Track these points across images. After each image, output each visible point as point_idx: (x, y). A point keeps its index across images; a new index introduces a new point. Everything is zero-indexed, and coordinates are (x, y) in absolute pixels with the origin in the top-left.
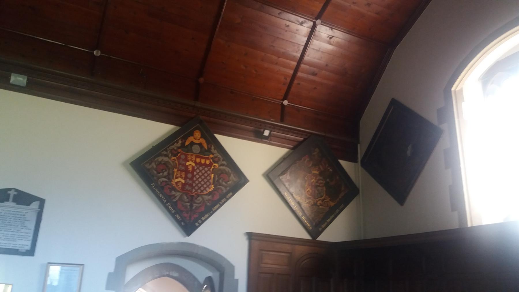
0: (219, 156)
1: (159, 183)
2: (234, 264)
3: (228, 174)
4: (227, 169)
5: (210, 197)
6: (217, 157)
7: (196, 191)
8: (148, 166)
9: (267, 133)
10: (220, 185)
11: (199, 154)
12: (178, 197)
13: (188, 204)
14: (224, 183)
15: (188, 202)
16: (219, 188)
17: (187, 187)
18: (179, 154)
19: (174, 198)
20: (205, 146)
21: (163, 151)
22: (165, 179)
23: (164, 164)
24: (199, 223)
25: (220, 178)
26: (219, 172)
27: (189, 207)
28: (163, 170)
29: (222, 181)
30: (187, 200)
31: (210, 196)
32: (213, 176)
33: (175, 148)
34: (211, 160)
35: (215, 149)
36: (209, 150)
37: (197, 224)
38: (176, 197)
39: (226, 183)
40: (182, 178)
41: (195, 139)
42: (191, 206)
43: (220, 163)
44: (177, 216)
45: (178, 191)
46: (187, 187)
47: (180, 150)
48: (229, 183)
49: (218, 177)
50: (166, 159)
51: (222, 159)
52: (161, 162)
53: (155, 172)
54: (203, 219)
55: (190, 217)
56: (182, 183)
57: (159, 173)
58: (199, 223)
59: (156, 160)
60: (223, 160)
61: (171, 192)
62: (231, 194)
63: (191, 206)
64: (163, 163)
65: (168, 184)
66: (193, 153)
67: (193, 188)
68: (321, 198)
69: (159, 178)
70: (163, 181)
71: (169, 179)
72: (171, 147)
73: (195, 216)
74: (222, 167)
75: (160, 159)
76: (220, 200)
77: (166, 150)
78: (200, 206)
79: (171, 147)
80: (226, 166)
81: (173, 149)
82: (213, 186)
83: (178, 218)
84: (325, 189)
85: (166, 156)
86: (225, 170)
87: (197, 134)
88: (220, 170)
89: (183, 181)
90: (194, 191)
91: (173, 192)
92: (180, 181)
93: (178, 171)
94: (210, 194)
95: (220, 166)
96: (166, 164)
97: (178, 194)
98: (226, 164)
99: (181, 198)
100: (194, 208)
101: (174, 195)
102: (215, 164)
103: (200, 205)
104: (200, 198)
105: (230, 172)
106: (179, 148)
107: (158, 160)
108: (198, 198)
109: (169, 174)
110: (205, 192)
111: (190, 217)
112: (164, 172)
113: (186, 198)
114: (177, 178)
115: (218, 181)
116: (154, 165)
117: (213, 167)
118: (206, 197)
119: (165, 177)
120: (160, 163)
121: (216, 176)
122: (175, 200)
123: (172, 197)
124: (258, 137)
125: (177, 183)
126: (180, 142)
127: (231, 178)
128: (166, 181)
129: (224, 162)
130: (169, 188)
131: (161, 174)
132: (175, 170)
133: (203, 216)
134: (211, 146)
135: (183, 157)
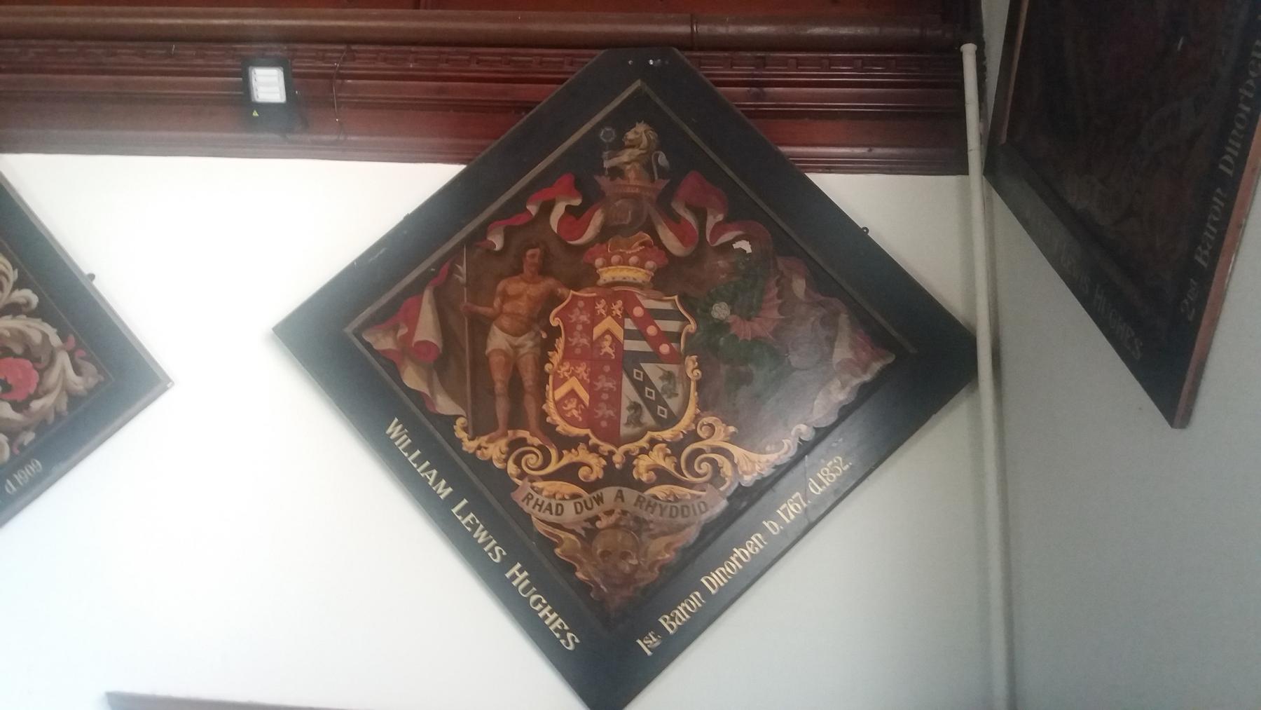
3: (39, 359)
4: (36, 330)
9: (268, 84)
39: (16, 406)
48: (36, 405)
51: (13, 275)
60: (19, 285)
62: (36, 466)
68: (667, 434)
80: (32, 314)
84: (693, 373)
86: (21, 336)
98: (35, 300)
105: (55, 340)
124: (225, 120)
127: (53, 377)
129: (27, 295)
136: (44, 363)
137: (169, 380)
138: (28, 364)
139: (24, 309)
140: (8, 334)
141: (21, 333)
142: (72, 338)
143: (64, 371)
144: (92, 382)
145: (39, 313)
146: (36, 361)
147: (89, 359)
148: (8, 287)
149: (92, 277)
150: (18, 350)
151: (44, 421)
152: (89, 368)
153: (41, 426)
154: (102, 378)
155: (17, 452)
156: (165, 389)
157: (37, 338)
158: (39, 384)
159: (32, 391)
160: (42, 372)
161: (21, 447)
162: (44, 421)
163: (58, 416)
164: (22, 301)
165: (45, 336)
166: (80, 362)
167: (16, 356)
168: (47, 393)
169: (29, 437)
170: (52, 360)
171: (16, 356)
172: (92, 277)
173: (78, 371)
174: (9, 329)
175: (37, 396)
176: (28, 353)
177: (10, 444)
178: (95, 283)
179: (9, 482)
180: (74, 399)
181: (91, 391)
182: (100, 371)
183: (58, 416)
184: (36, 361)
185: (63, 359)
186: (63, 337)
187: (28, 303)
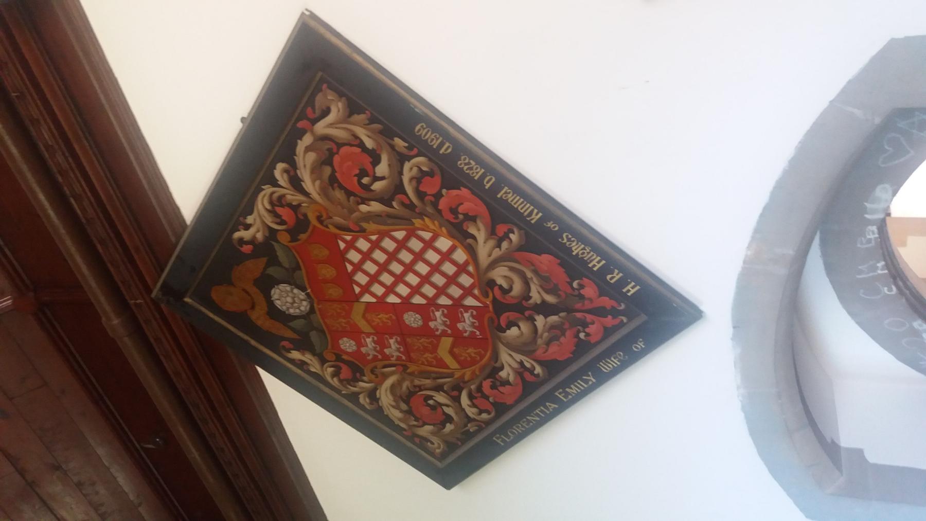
0: (262, 203)
1: (484, 416)
2: (889, 38)
3: (329, 150)
4: (305, 160)
5: (479, 232)
6: (272, 212)
7: (468, 292)
8: (437, 445)
10: (399, 188)
11: (303, 289)
12: (519, 357)
13: (540, 320)
14: (382, 169)
15: (532, 320)
16: (421, 195)
17: (467, 324)
18: (345, 357)
19: (531, 371)
20: (255, 267)
21: (362, 407)
22: (465, 400)
23: (407, 402)
24: (622, 283)
25: (367, 188)
26: (339, 194)
27: (554, 319)
28: (429, 405)
29: (376, 179)
30: (525, 327)
31: (472, 230)
32: (370, 226)
33: (330, 370)
34: (303, 237)
35: (247, 227)
36: (265, 249)
37: (631, 289)
38: (521, 363)
39: (376, 161)
40: (435, 348)
41: (253, 308)
42: (545, 309)
43: (293, 197)
44: (605, 368)
45: (496, 356)
46: (467, 324)
47: (329, 356)
48: (369, 144)
49: (364, 201)
50: (385, 398)
51: (268, 189)
52: (402, 411)
53: (449, 427)
54: (596, 263)
55: (600, 312)
56: (453, 345)
57: (449, 419)
58: (622, 283)
59: (403, 425)
60: (274, 183)
61: (506, 383)
63: (545, 309)
64: (404, 406)
65: (479, 389)
66: (312, 310)
67: (457, 303)
69: (470, 420)
70: (474, 405)
71: (458, 388)
72: (335, 382)
73: (590, 291)
74: (308, 184)
75: (395, 414)
76: (476, 187)
77: (354, 397)
78: (536, 272)
79: (335, 382)
81: (335, 374)
82: (417, 222)
83: (614, 362)
85: (372, 395)
86: (315, 170)
87: (229, 298)
88: (324, 192)
89: (447, 342)
90: (470, 301)
91: (503, 374)
92: (451, 352)
93: (410, 359)
94: (461, 236)
95: (306, 194)
96: (406, 398)
97: (509, 360)
98: (280, 166)
99: (526, 348)
100: (550, 299)
101: (517, 372)
102: (314, 222)
103: (529, 274)
104: (500, 275)
105: (307, 140)
106: (323, 361)
107: (400, 420)
108: (500, 281)
109: (439, 388)
110: (460, 256)
111: (600, 312)
112: (441, 405)
113: (514, 331)
114: (441, 364)
115: (386, 200)
116: (426, 430)
117: (333, 230)
118: (484, 249)
119: (457, 399)
120: (409, 412)
121: (364, 208)
122: (538, 370)
123: (527, 376)
125: (463, 364)
126: (295, 355)
127: (339, 134)
128: (471, 397)
130: (493, 387)
131: (449, 411)
132: (412, 368)
133: (584, 263)
134: (241, 241)
135: (348, 345)
136: (328, 145)
137: (303, 14)
138: (336, 159)
139: (292, 173)
140: (318, 183)
141: (313, 171)
142: (300, 125)
143: (331, 125)
144: (331, 96)
145: (289, 157)
146: (331, 153)
147: (311, 102)
148: (281, 191)
149: (243, 120)
150: (327, 170)
151: (381, 132)
152: (319, 100)
153: (387, 133)
154: (325, 86)
155: (415, 151)
156: (313, 16)
157: (312, 156)
158: (351, 145)
159: (358, 150)
160: (340, 145)
161: (410, 148)
162: (381, 132)
163: (372, 120)
164: (285, 175)
165: (308, 149)
166: (318, 113)
167: (334, 171)
168: (356, 137)
169: (399, 143)
170: (326, 138)
171: (334, 171)
172: (243, 120)
173: (326, 112)
174: (313, 182)
175: (361, 145)
176: (327, 160)
177: (409, 158)
178: (245, 115)
179: (441, 152)
180: (353, 109)
181: (341, 95)
182: (318, 90)
183: (372, 120)
184: (331, 153)
185: (321, 127)
186: (301, 134)
187: (286, 171)
